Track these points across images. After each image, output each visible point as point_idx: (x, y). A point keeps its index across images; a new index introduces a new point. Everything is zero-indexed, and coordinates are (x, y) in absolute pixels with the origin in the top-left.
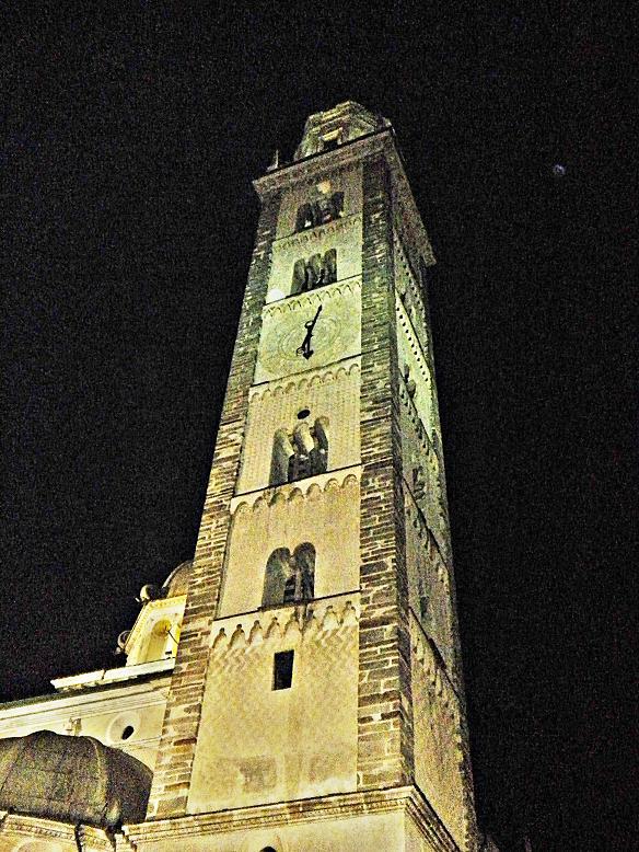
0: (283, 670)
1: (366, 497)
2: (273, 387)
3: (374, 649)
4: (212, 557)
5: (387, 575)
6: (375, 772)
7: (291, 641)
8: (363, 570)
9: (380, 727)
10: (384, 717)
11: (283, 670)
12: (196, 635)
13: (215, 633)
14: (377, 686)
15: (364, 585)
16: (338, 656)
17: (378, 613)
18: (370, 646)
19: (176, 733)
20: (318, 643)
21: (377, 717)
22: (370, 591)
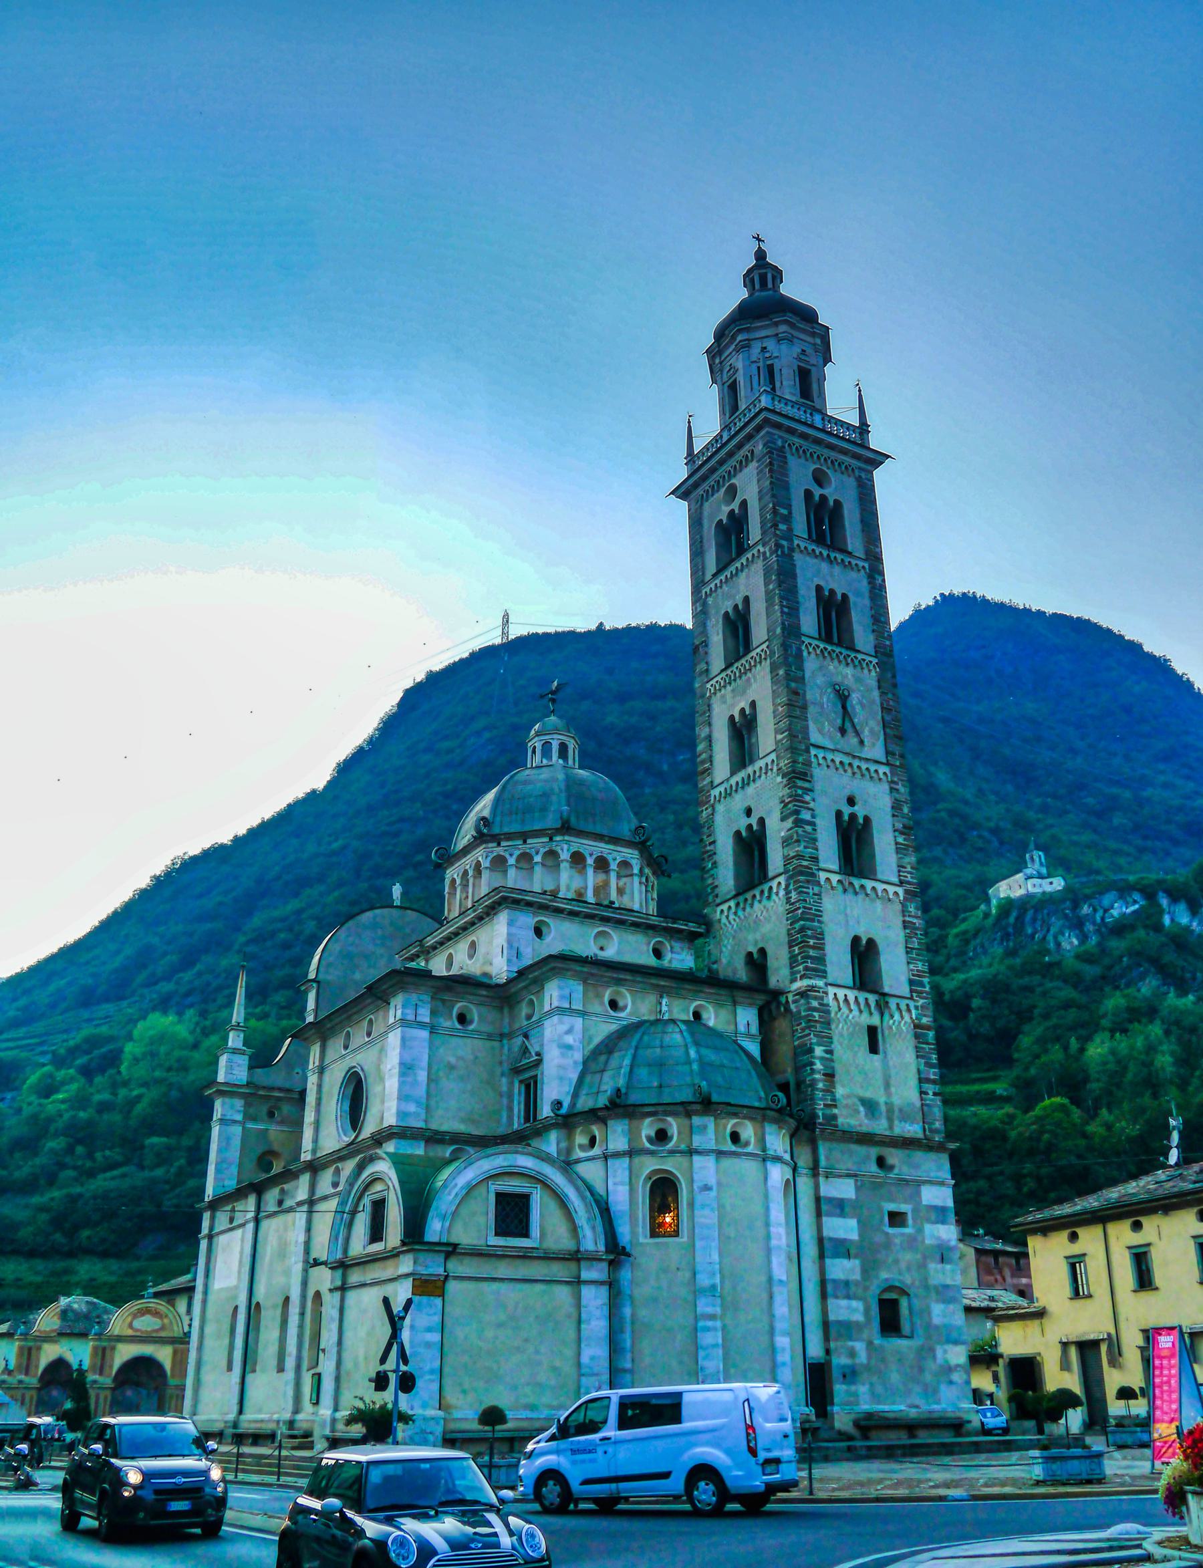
0: (873, 1039)
1: (907, 919)
2: (830, 756)
3: (924, 1046)
4: (816, 924)
5: (926, 992)
6: (933, 1127)
7: (875, 1020)
8: (911, 982)
9: (932, 1100)
10: (935, 1094)
11: (873, 1039)
12: (819, 992)
13: (831, 996)
14: (929, 1073)
15: (914, 995)
16: (903, 1040)
17: (924, 1020)
18: (923, 1043)
19: (822, 1067)
20: (891, 1028)
21: (931, 1093)
22: (917, 1001)
